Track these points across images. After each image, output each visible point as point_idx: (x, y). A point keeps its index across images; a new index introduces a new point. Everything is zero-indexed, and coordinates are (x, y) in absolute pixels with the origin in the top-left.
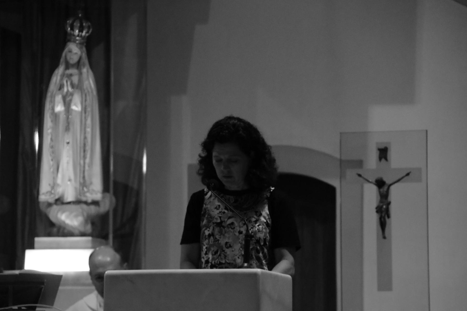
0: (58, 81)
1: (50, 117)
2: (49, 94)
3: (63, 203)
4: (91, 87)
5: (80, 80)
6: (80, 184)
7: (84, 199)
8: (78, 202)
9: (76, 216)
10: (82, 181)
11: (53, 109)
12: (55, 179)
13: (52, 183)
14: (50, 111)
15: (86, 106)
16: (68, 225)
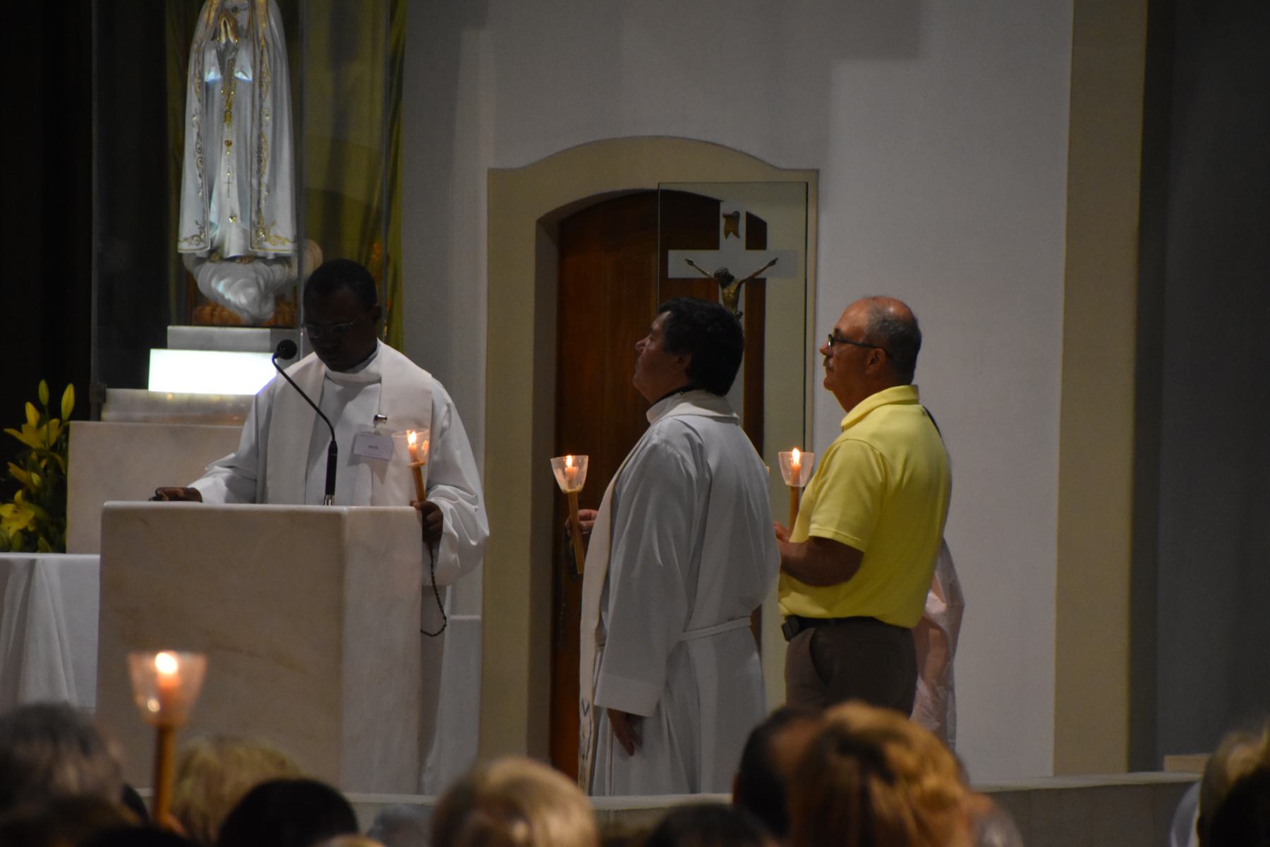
0: (211, 21)
1: (196, 91)
2: (195, 46)
4: (272, 34)
5: (252, 21)
6: (252, 224)
7: (260, 253)
8: (248, 258)
9: (245, 286)
11: (201, 77)
12: (205, 211)
13: (200, 222)
14: (196, 81)
15: (261, 72)
16: (229, 301)
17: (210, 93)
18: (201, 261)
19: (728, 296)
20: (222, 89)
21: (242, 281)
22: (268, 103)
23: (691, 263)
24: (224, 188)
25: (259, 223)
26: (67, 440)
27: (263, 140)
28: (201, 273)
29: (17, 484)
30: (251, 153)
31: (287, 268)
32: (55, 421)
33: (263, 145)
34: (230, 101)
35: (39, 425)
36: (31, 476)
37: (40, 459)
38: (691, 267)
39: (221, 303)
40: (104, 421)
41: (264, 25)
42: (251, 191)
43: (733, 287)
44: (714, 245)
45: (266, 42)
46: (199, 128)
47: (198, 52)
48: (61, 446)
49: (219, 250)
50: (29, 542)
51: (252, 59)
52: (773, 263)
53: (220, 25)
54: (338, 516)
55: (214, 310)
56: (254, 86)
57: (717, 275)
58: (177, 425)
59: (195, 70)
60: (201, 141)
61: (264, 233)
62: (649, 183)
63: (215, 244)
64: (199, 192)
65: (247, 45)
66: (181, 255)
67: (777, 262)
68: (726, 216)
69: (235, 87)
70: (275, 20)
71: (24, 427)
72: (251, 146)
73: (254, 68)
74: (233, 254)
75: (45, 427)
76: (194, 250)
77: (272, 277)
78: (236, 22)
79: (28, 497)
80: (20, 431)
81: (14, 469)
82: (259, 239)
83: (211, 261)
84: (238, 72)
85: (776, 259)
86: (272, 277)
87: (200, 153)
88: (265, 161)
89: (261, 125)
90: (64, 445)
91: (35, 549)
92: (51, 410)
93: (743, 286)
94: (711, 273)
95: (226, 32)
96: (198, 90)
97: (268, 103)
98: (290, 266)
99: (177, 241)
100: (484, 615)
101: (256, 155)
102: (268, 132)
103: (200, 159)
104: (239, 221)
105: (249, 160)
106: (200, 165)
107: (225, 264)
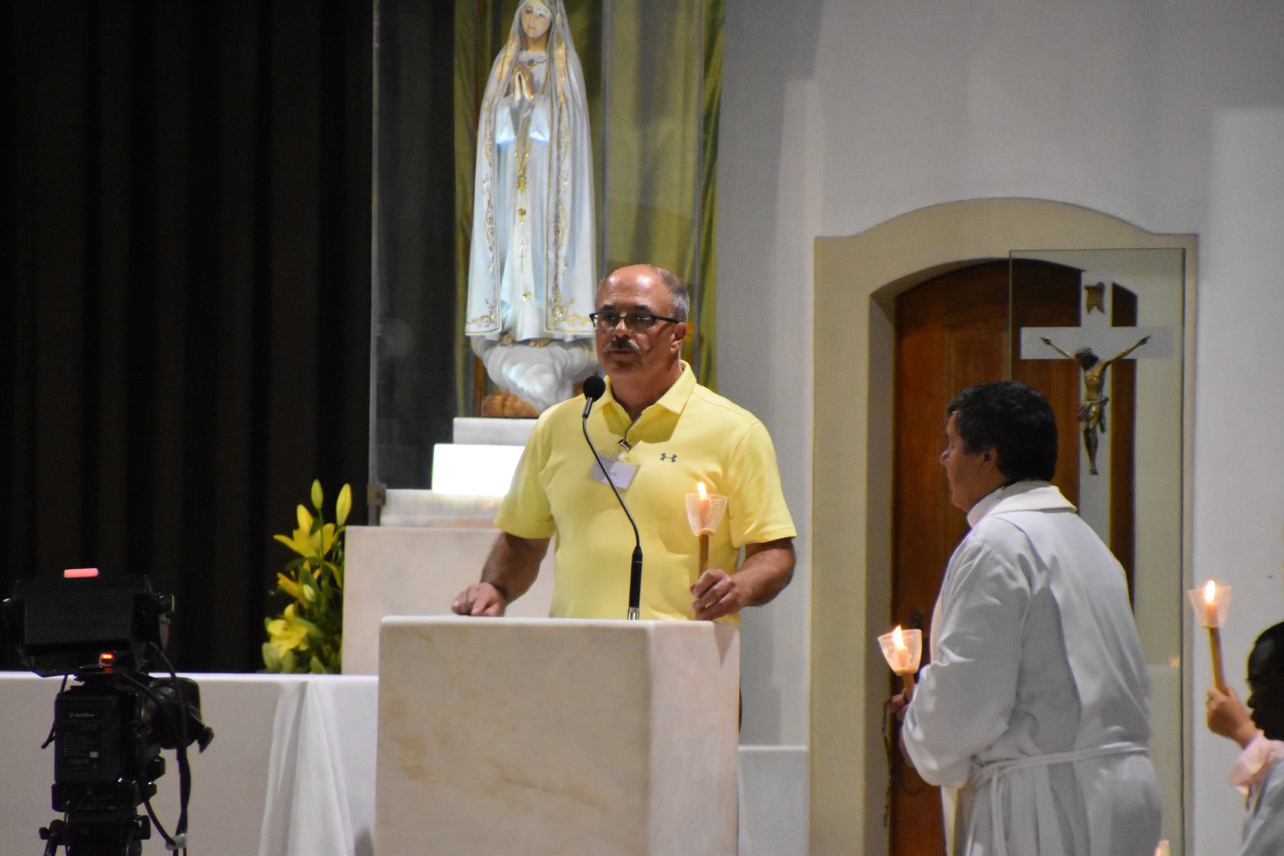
0: (504, 76)
1: (486, 154)
2: (485, 104)
3: (515, 342)
5: (550, 75)
6: (548, 302)
7: (557, 335)
8: (545, 341)
9: (540, 372)
10: (550, 295)
11: (493, 138)
12: (496, 289)
13: (491, 301)
14: (488, 142)
15: (559, 131)
16: (522, 389)
17: (502, 155)
18: (491, 344)
19: (1092, 379)
20: (516, 151)
21: (536, 366)
22: (566, 165)
23: (1047, 342)
24: (517, 262)
25: (555, 301)
26: (343, 547)
27: (561, 207)
28: (491, 358)
29: (287, 599)
30: (548, 223)
31: (587, 351)
32: (330, 527)
33: (562, 215)
34: (524, 165)
35: (312, 532)
36: (302, 589)
37: (313, 569)
38: (1049, 347)
39: (513, 392)
40: (384, 525)
41: (563, 79)
42: (548, 264)
43: (1096, 370)
44: (1074, 321)
45: (566, 100)
46: (490, 195)
47: (490, 110)
48: (337, 555)
49: (511, 332)
50: (301, 662)
51: (549, 115)
52: (1144, 341)
53: (514, 80)
54: (641, 633)
55: (505, 400)
56: (551, 147)
57: (1078, 356)
58: (464, 530)
59: (486, 130)
60: (492, 209)
61: (562, 312)
62: (999, 250)
63: (506, 326)
64: (489, 267)
65: (545, 99)
66: (468, 339)
67: (1149, 340)
68: (1089, 288)
69: (530, 148)
70: (575, 75)
71: (295, 533)
72: (548, 214)
73: (552, 127)
74: (526, 336)
75: (318, 533)
76: (484, 332)
77: (569, 362)
78: (531, 76)
79: (301, 612)
80: (291, 537)
81: (283, 581)
82: (556, 319)
83: (503, 345)
84: (533, 131)
85: (1148, 338)
86: (569, 362)
87: (491, 223)
88: (563, 231)
89: (558, 192)
90: (340, 554)
91: (308, 671)
92: (326, 514)
93: (1109, 369)
94: (1071, 353)
95: (521, 88)
96: (489, 153)
97: (566, 165)
98: (590, 349)
99: (465, 322)
100: (812, 746)
101: (554, 224)
102: (566, 198)
103: (490, 230)
104: (534, 299)
105: (545, 230)
106: (490, 236)
107: (518, 348)
